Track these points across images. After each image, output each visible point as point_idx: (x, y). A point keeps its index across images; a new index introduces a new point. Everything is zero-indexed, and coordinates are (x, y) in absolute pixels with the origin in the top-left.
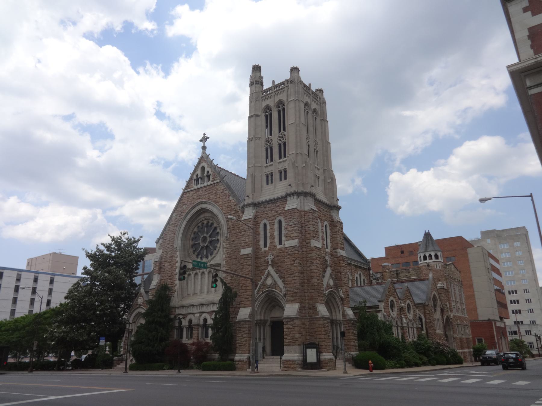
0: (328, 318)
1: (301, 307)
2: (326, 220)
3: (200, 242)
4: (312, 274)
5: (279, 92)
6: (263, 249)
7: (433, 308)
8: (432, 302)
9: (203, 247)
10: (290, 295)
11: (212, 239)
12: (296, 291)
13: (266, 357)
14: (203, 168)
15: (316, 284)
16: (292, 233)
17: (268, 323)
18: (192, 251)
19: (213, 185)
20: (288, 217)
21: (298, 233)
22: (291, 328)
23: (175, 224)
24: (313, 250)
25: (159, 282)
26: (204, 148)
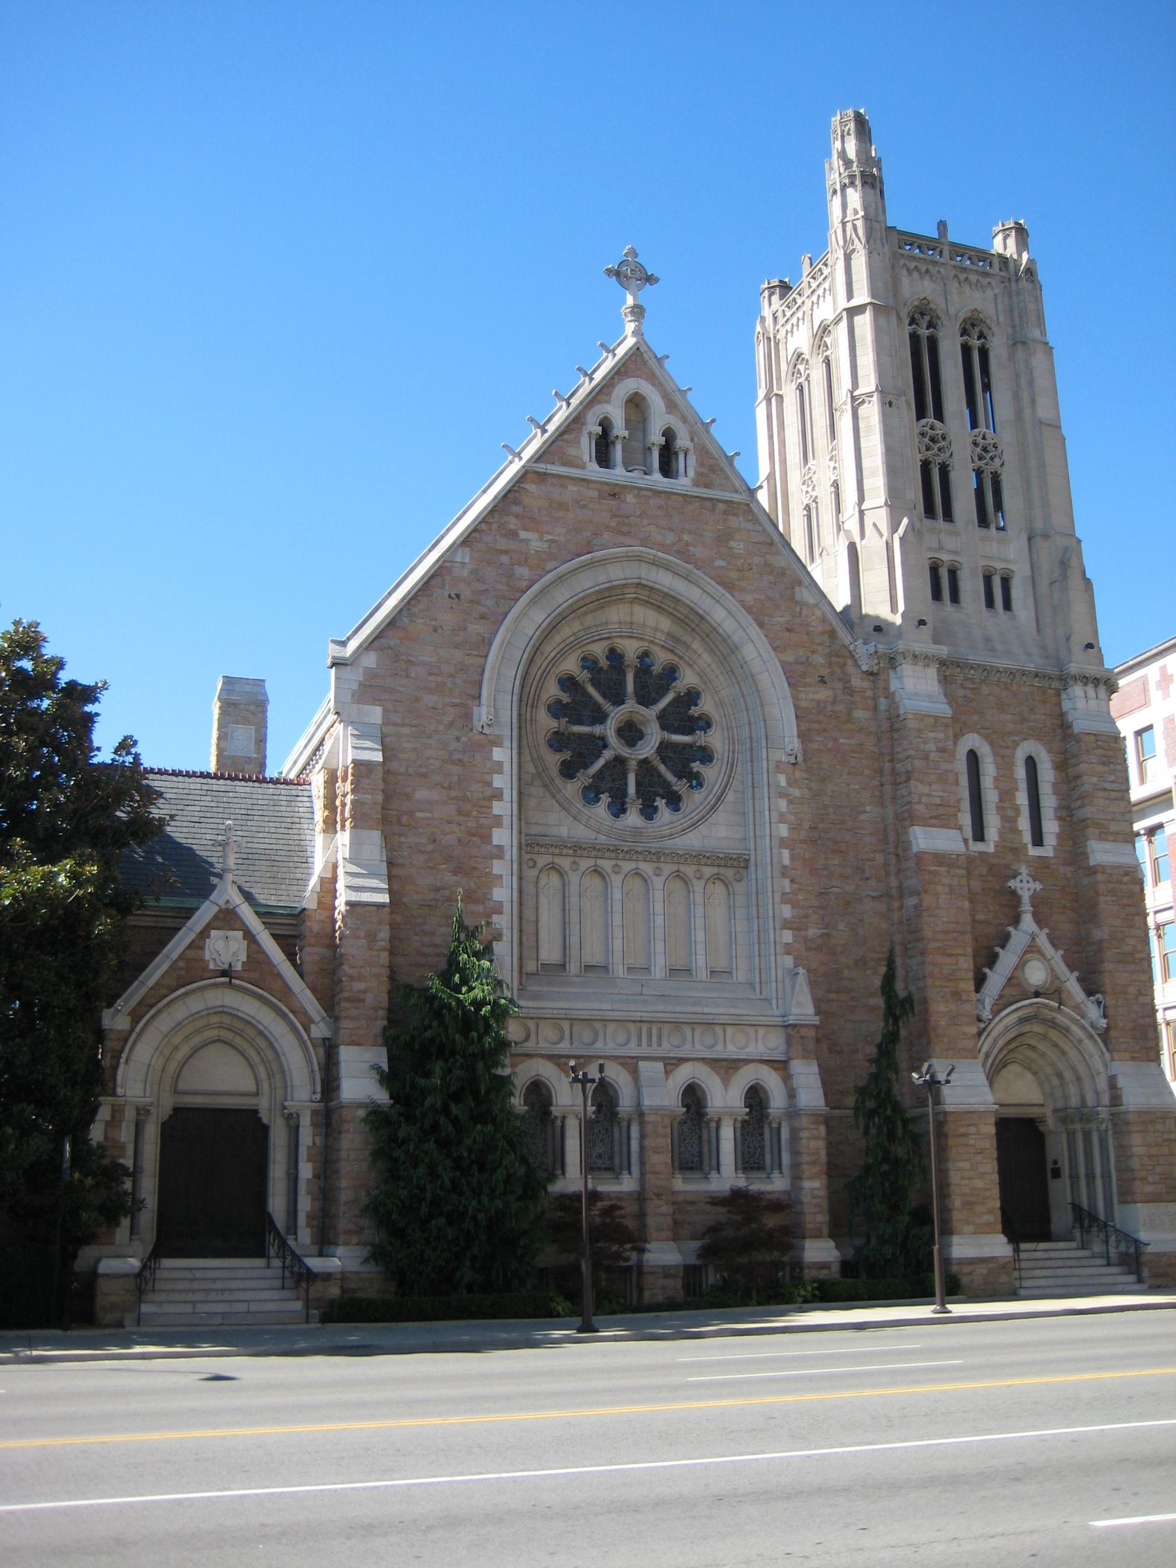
14: (636, 403)
19: (709, 504)
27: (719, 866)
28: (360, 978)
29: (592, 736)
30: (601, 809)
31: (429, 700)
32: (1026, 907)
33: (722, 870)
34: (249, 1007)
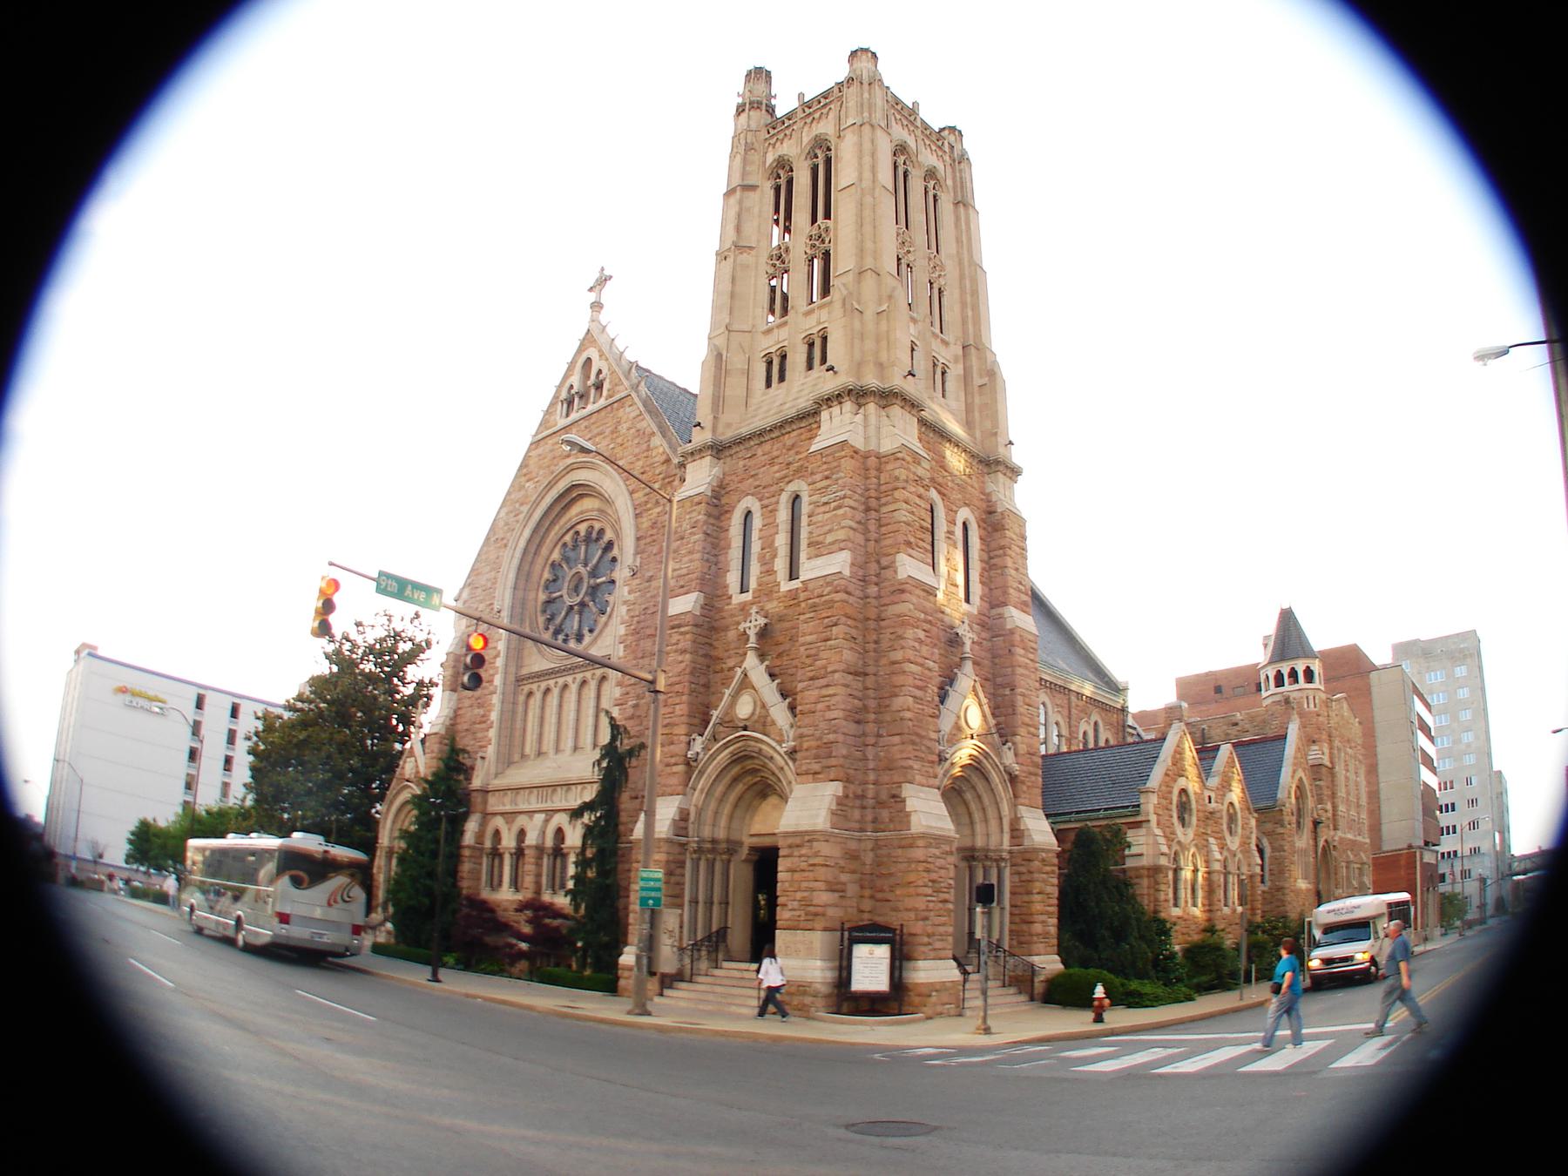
0: (946, 840)
1: (847, 796)
2: (967, 505)
3: (564, 592)
4: (899, 680)
5: (817, 116)
6: (738, 599)
7: (1294, 819)
8: (1293, 800)
9: (571, 608)
10: (808, 753)
11: (599, 581)
12: (831, 737)
13: (726, 964)
15: (908, 715)
16: (830, 531)
17: (745, 852)
18: (541, 619)
20: (818, 477)
21: (851, 528)
22: (803, 871)
23: (503, 539)
24: (903, 591)
25: (451, 715)
26: (597, 306)
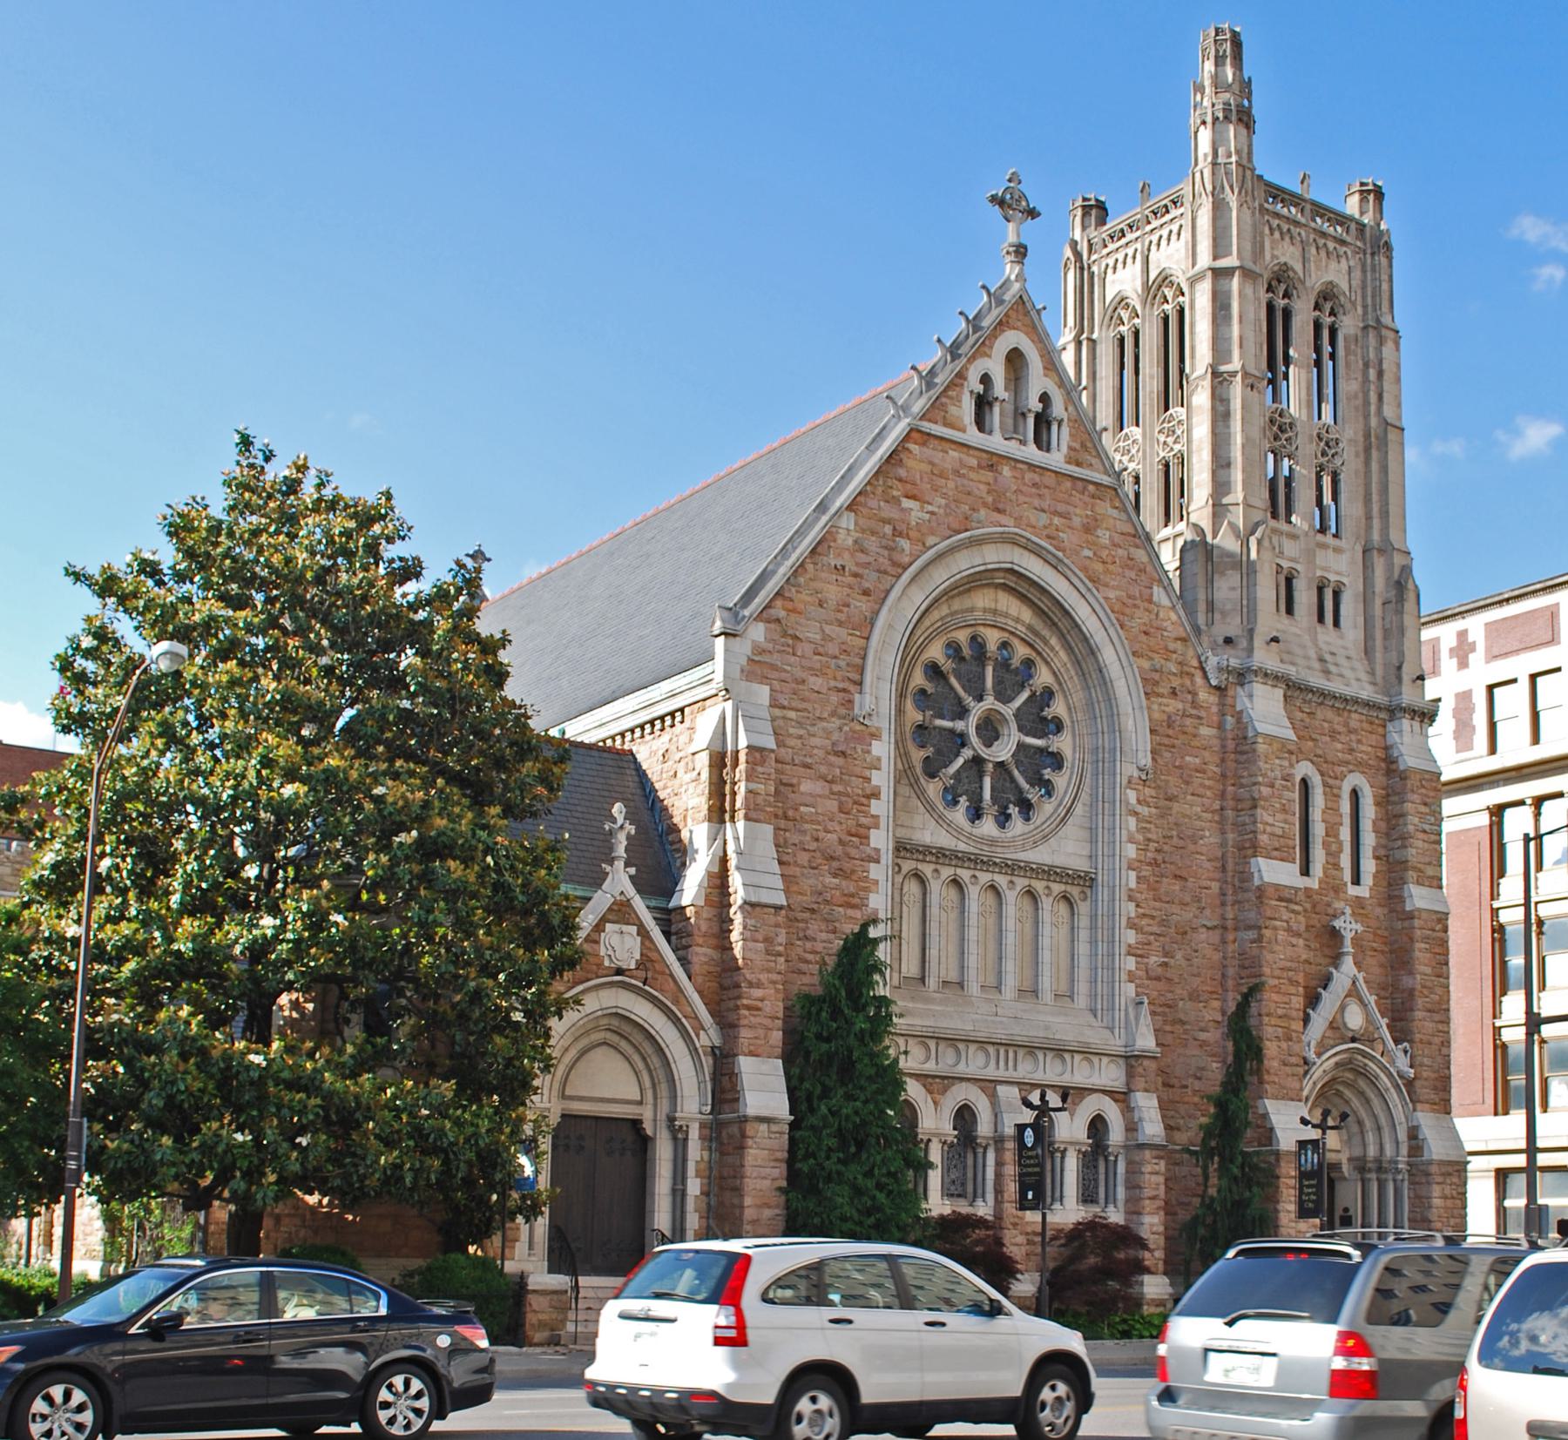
19: (1080, 484)
27: (1067, 883)
28: (759, 985)
29: (952, 731)
30: (959, 815)
31: (816, 682)
32: (1348, 947)
33: (1069, 888)
34: (642, 1011)
